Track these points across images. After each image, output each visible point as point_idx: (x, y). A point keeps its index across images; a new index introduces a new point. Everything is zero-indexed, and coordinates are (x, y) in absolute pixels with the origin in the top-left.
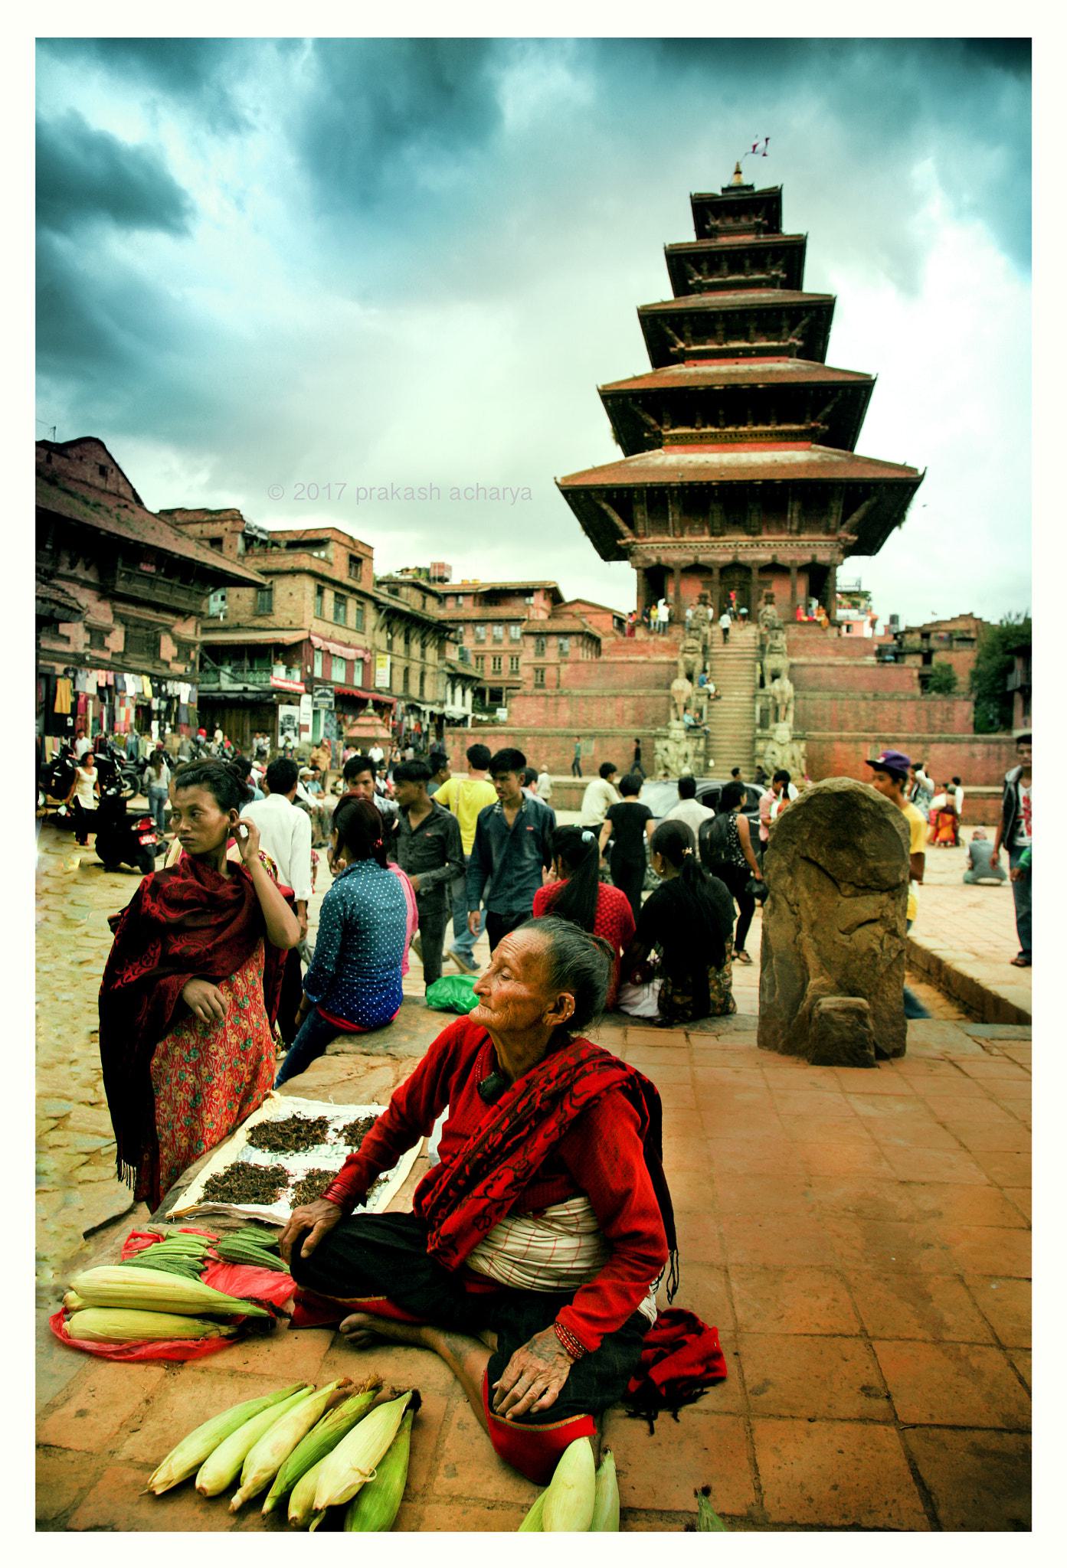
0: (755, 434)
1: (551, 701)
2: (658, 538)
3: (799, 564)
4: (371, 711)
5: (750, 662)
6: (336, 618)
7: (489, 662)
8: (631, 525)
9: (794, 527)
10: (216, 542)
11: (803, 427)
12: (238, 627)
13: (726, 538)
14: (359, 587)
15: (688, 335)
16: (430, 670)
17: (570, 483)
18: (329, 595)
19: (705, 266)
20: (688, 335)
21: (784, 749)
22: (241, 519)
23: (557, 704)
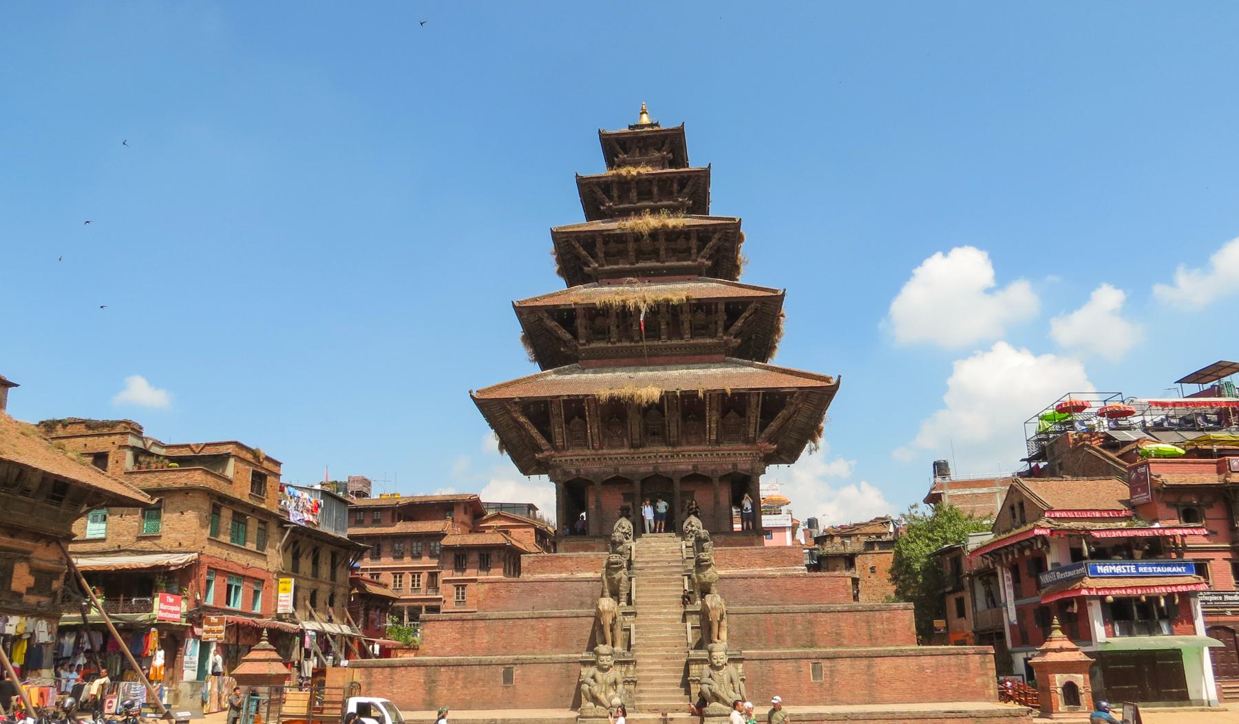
0: (670, 347)
2: (578, 451)
3: (721, 473)
4: (265, 643)
6: (233, 540)
7: (408, 578)
8: (548, 437)
9: (713, 437)
10: (100, 459)
11: (715, 341)
12: (119, 551)
14: (263, 506)
15: (601, 255)
16: (340, 591)
17: (486, 396)
18: (226, 514)
19: (615, 193)
22: (137, 432)
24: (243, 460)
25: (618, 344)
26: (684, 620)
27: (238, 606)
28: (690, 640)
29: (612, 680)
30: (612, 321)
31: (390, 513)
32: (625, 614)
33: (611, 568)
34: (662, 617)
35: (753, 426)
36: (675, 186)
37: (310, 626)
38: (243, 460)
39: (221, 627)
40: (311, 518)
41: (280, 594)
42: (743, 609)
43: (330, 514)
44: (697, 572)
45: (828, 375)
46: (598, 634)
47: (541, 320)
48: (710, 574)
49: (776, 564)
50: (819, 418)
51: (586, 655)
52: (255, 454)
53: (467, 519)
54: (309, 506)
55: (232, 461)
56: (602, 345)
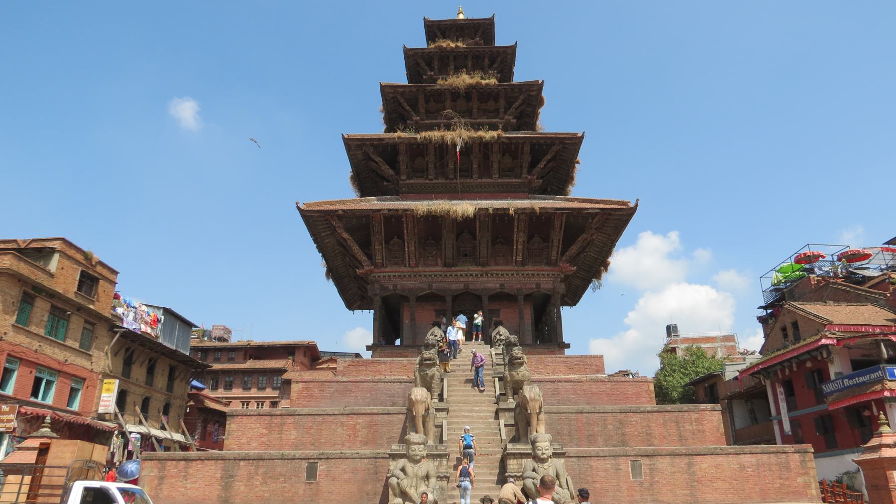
1: (277, 420)
5: (490, 378)
9: (519, 259)
13: (457, 268)
14: (91, 307)
15: (422, 111)
16: (176, 403)
19: (436, 64)
21: (546, 465)
23: (282, 424)
24: (70, 258)
26: (497, 417)
27: (49, 401)
28: (504, 437)
29: (424, 473)
30: (431, 158)
31: (243, 353)
32: (438, 410)
33: (424, 364)
34: (474, 414)
35: (555, 249)
36: (487, 61)
37: (134, 429)
38: (70, 258)
39: (12, 417)
40: (149, 330)
41: (103, 395)
43: (172, 331)
44: (510, 370)
45: (627, 200)
46: (411, 422)
47: (368, 158)
48: (523, 372)
49: (579, 372)
50: (609, 253)
51: (395, 448)
52: (87, 257)
53: (306, 361)
54: (149, 319)
55: (56, 256)
56: (420, 181)
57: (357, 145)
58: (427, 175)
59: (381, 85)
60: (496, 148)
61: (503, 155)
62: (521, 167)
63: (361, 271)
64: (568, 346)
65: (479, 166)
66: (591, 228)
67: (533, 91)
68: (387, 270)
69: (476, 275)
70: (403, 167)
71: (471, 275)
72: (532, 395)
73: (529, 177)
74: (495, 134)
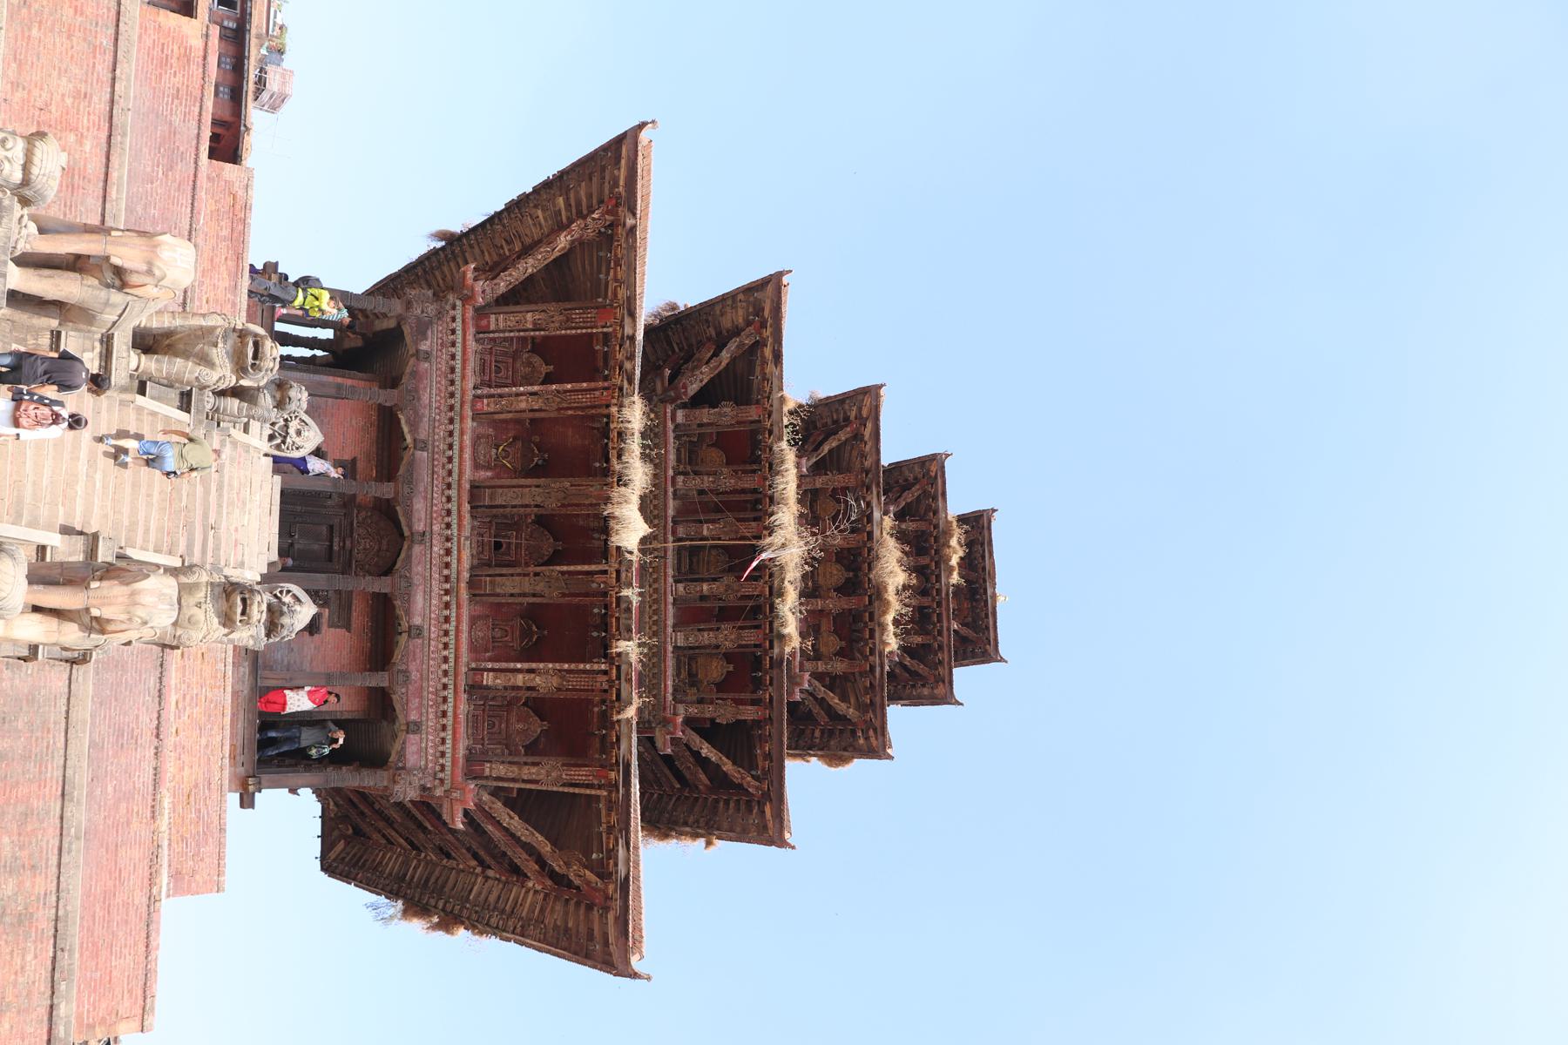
5: (182, 549)
9: (488, 679)
13: (467, 516)
15: (819, 482)
19: (909, 526)
20: (819, 482)
25: (671, 490)
30: (727, 481)
35: (513, 771)
36: (918, 639)
42: (83, 711)
57: (759, 311)
58: (685, 474)
59: (881, 386)
60: (750, 637)
61: (728, 657)
62: (700, 701)
63: (470, 275)
64: (247, 802)
65: (703, 598)
66: (567, 864)
67: (867, 739)
68: (470, 337)
69: (447, 565)
70: (705, 415)
71: (448, 552)
72: (147, 599)
73: (680, 720)
74: (791, 627)
